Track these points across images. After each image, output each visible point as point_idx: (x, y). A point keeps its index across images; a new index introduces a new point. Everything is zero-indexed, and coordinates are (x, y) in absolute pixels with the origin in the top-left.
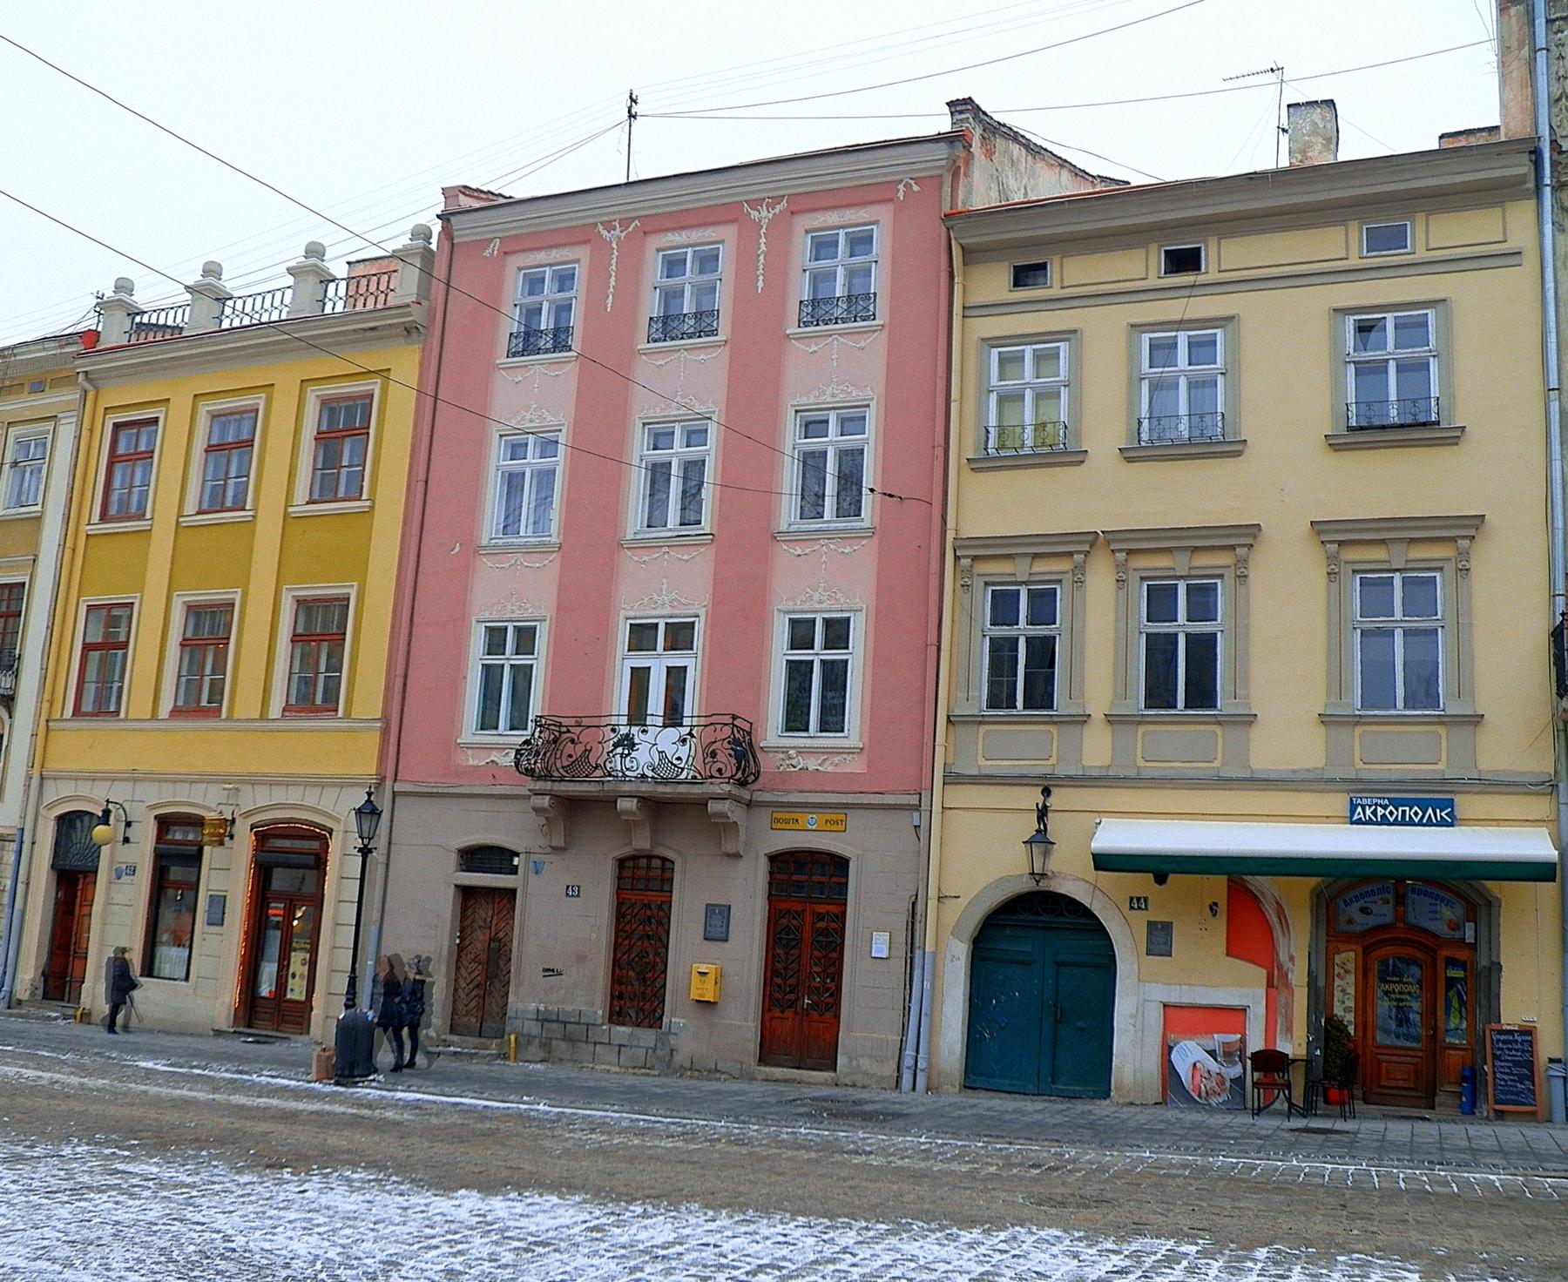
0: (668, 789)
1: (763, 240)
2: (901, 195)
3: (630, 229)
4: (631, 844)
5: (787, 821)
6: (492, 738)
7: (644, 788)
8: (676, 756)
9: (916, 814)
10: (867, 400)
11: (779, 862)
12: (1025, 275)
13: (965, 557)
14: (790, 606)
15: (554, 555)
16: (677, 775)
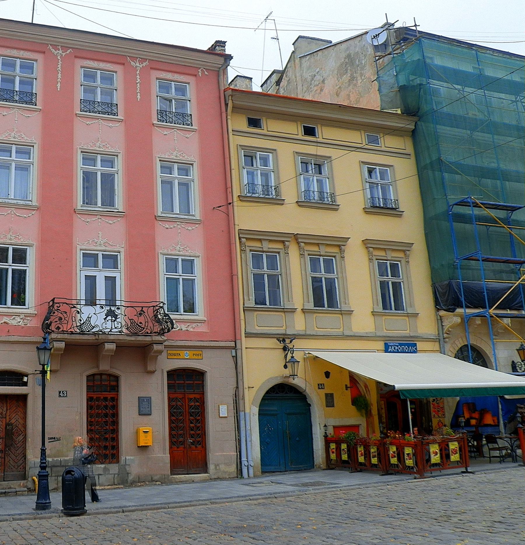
0: (133, 338)
1: (138, 77)
2: (200, 74)
3: (68, 52)
4: (98, 367)
5: (175, 355)
6: (4, 309)
7: (121, 337)
8: (139, 322)
9: (234, 351)
10: (193, 161)
11: (173, 374)
12: (254, 123)
13: (244, 238)
14: (165, 251)
15: (33, 213)
16: (140, 331)
